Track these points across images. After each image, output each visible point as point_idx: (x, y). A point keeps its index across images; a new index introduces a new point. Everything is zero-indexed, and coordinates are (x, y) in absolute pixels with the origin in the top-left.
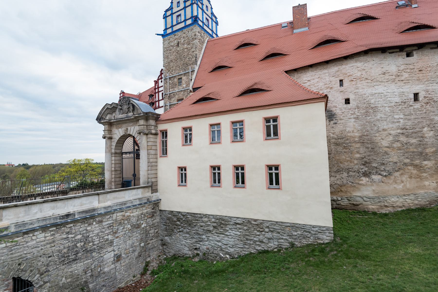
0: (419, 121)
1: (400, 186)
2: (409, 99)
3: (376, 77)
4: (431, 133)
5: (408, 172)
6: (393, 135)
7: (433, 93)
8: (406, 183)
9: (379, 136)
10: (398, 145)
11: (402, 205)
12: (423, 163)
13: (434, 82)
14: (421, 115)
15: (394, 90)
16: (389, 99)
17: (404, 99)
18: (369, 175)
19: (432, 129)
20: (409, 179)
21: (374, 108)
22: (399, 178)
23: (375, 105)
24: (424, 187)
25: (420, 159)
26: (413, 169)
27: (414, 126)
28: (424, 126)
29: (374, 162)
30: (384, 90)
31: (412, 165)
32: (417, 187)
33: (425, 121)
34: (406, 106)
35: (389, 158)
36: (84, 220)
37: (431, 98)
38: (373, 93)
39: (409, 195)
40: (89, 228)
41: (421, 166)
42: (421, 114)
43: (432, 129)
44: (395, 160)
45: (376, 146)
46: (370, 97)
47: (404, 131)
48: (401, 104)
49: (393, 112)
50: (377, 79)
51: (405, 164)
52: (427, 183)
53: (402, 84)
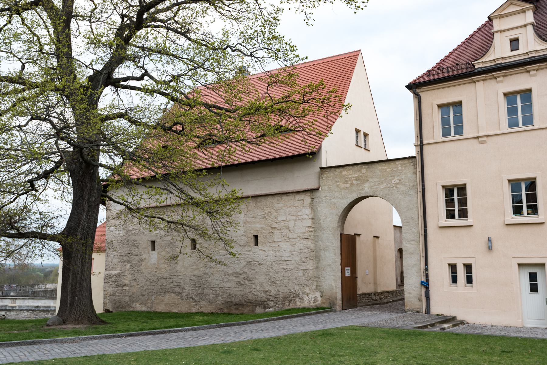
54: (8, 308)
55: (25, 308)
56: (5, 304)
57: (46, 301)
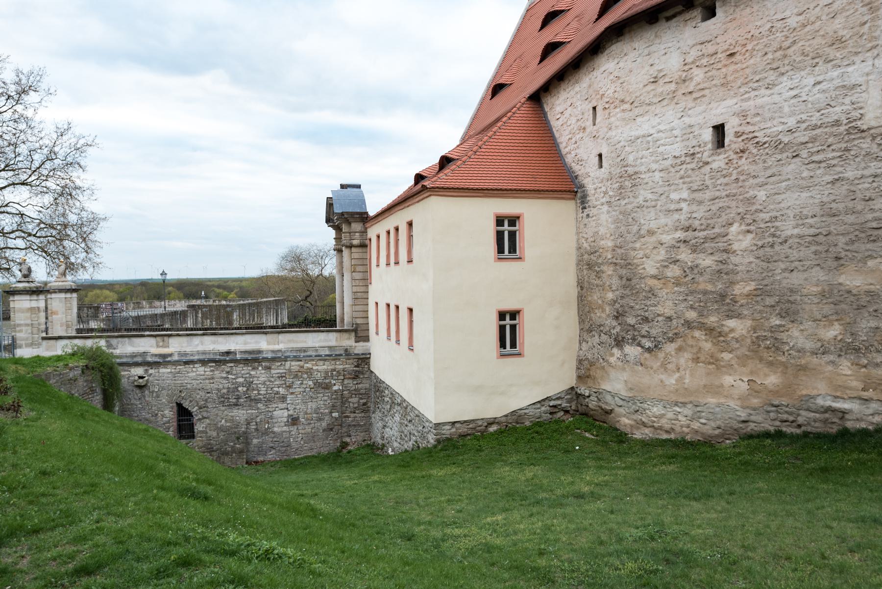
0: (721, 205)
1: (671, 381)
2: (702, 145)
3: (638, 94)
4: (747, 241)
5: (692, 346)
6: (666, 245)
7: (758, 119)
8: (684, 372)
9: (641, 249)
10: (674, 271)
11: (670, 426)
12: (724, 323)
13: (760, 84)
14: (726, 188)
15: (672, 124)
16: (662, 149)
17: (690, 146)
18: (622, 343)
19: (748, 228)
20: (690, 363)
21: (633, 177)
22: (674, 359)
23: (636, 169)
24: (716, 390)
25: (718, 313)
26: (703, 337)
27: (709, 221)
28: (731, 221)
29: (630, 314)
30: (653, 127)
31: (702, 326)
32: (705, 386)
33: (734, 204)
34: (693, 166)
35: (656, 306)
36: (246, 361)
37: (751, 136)
38: (633, 138)
39: (684, 404)
40: (253, 373)
41: (720, 333)
42: (726, 184)
43: (748, 228)
44: (668, 312)
45: (635, 274)
46: (627, 149)
47: (690, 234)
48: (685, 162)
49: (667, 183)
50: (642, 97)
51: (688, 324)
52: (728, 380)
53: (688, 102)
54: (149, 359)
55: (196, 358)
56: (141, 350)
57: (248, 338)
